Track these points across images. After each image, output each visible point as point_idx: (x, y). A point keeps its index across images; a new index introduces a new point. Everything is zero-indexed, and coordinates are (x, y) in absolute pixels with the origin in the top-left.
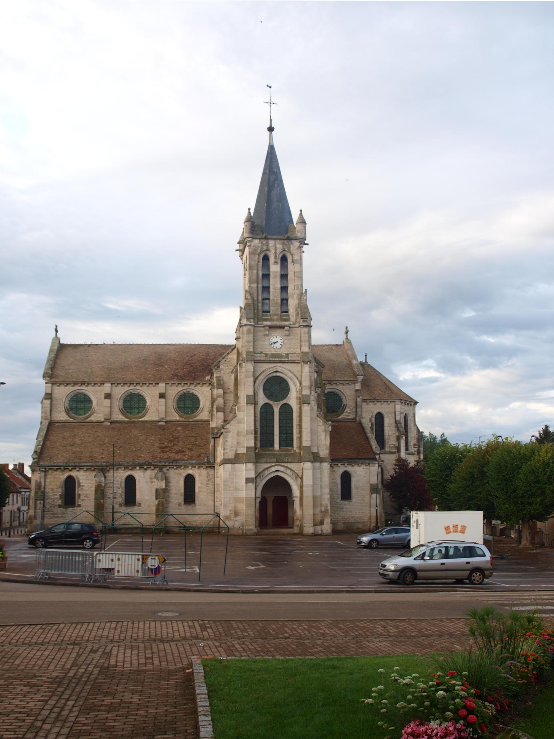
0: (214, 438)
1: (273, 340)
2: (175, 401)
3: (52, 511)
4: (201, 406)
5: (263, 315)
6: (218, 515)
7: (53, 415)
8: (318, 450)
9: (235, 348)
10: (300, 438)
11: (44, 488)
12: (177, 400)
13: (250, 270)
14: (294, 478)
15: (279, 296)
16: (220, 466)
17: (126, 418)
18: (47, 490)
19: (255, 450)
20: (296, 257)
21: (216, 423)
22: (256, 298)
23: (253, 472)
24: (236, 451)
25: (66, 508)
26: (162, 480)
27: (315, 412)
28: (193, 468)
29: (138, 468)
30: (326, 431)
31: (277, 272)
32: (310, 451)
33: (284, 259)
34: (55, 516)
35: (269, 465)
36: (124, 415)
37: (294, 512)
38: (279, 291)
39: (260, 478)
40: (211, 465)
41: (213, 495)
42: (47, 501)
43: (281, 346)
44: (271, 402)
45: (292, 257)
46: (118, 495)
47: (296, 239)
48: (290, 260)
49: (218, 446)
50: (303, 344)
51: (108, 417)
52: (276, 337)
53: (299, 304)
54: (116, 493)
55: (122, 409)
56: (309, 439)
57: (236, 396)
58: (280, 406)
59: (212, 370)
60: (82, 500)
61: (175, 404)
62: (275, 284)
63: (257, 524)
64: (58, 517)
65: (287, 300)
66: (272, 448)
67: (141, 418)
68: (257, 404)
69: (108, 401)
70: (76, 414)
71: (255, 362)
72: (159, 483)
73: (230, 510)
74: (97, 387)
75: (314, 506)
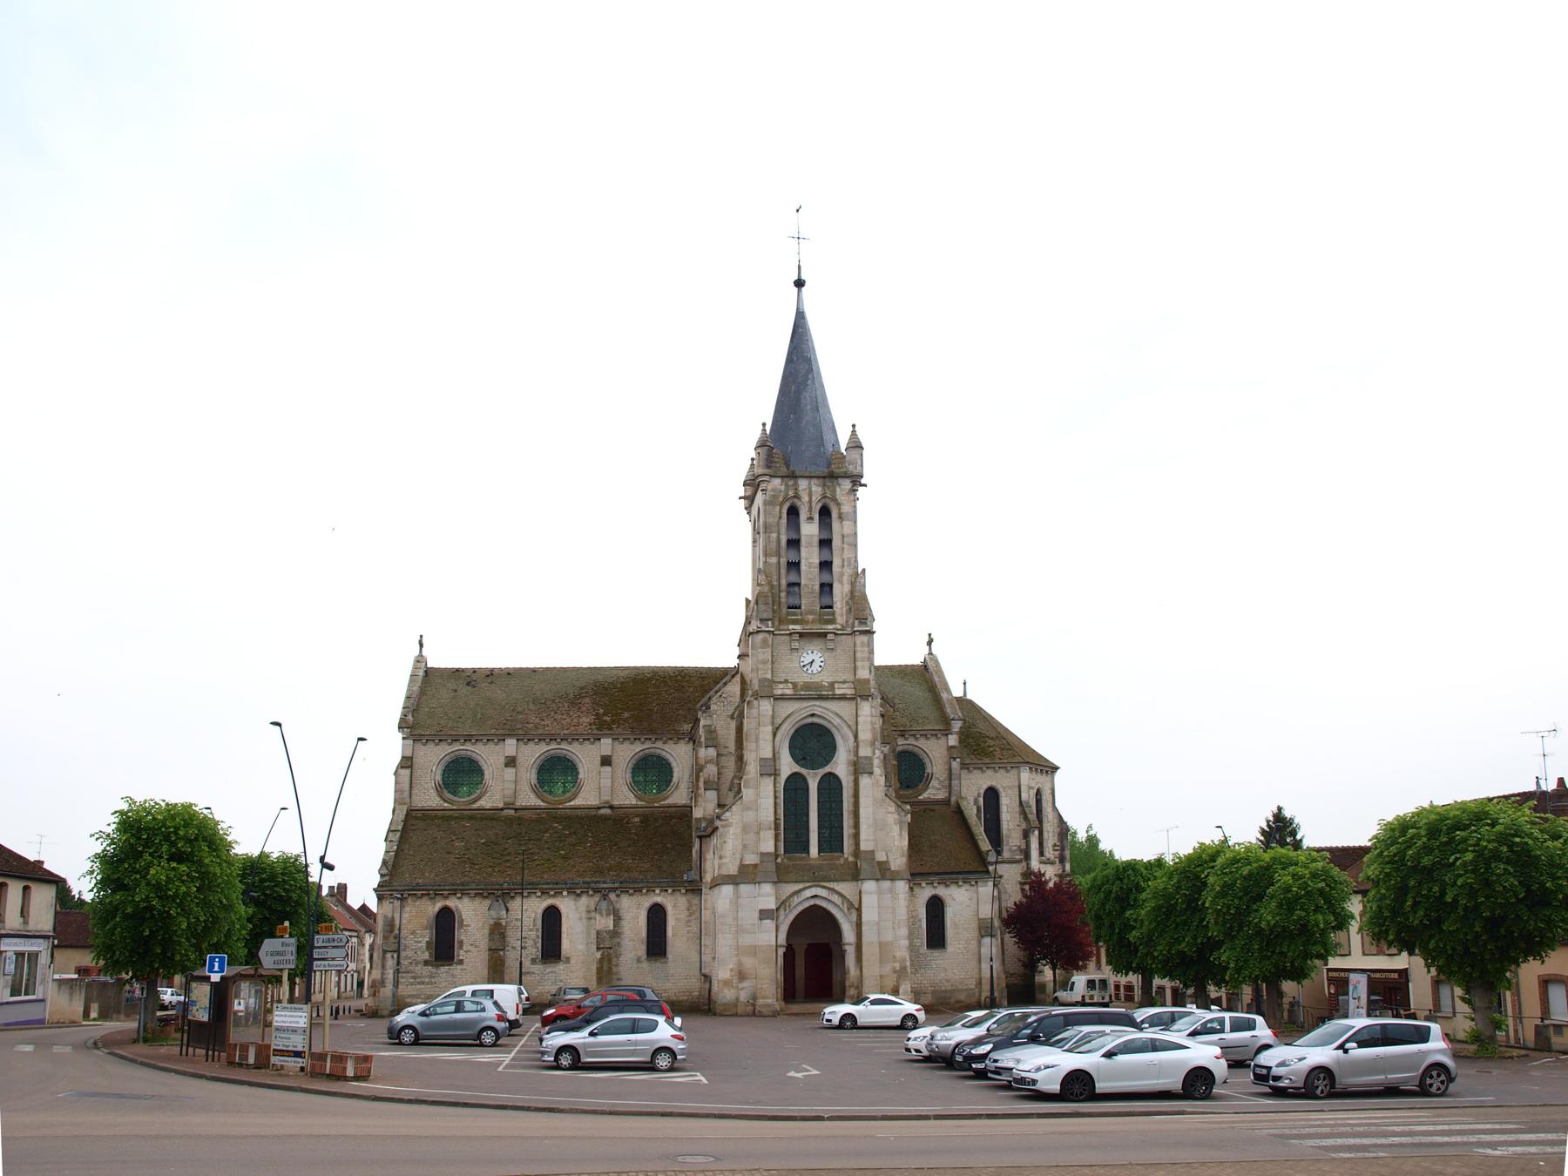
0: (701, 838)
1: (807, 659)
2: (629, 771)
3: (413, 972)
4: (675, 780)
5: (788, 614)
6: (707, 978)
7: (413, 797)
8: (887, 856)
9: (737, 672)
10: (856, 836)
11: (399, 929)
12: (633, 769)
13: (765, 532)
14: (846, 910)
15: (818, 579)
16: (710, 888)
17: (543, 801)
18: (404, 933)
19: (776, 859)
20: (846, 509)
21: (705, 811)
22: (775, 583)
23: (773, 899)
24: (741, 860)
25: (437, 966)
26: (608, 915)
27: (882, 789)
29: (565, 893)
30: (901, 823)
31: (812, 536)
32: (874, 859)
33: (825, 513)
34: (418, 980)
35: (801, 886)
36: (538, 796)
37: (844, 972)
38: (817, 570)
39: (785, 910)
40: (695, 888)
41: (698, 941)
42: (403, 954)
43: (820, 669)
44: (804, 771)
45: (840, 509)
46: (529, 943)
47: (846, 476)
48: (834, 515)
49: (708, 851)
50: (858, 664)
51: (511, 800)
52: (812, 652)
53: (852, 592)
54: (525, 938)
55: (535, 785)
56: (872, 838)
57: (740, 759)
58: (818, 781)
59: (696, 712)
60: (466, 951)
61: (629, 775)
62: (810, 556)
63: (779, 996)
64: (423, 983)
65: (831, 586)
66: (804, 855)
67: (569, 801)
68: (779, 775)
69: (511, 770)
70: (454, 793)
71: (775, 699)
72: (603, 921)
73: (731, 970)
74: (491, 746)
75: (881, 961)
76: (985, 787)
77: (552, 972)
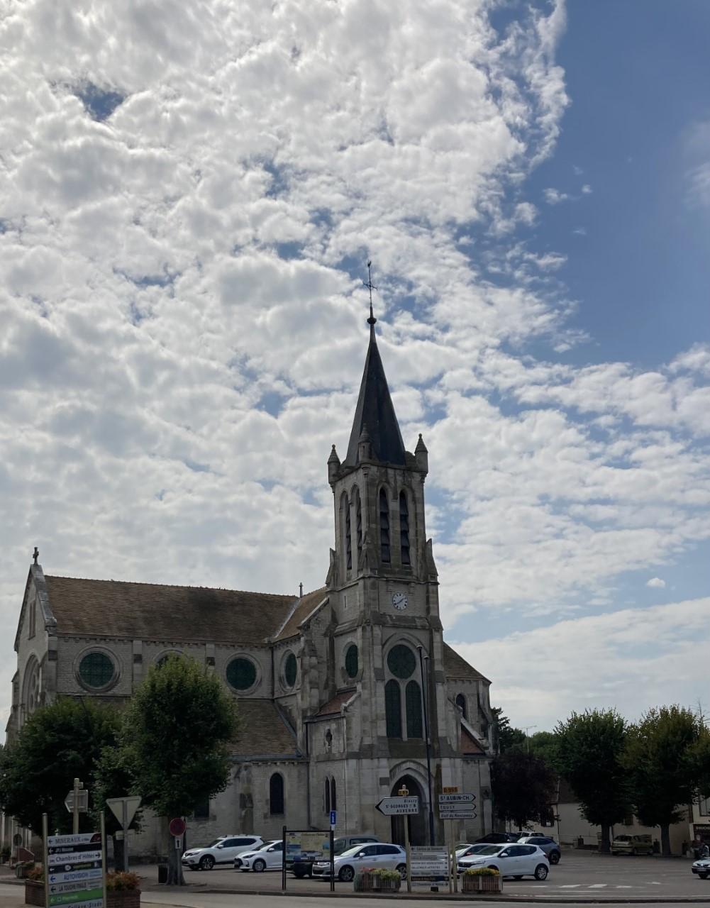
24: (361, 742)
28: (283, 765)
33: (403, 496)
44: (397, 679)
58: (406, 684)
62: (395, 527)
76: (457, 694)
77: (204, 827)
